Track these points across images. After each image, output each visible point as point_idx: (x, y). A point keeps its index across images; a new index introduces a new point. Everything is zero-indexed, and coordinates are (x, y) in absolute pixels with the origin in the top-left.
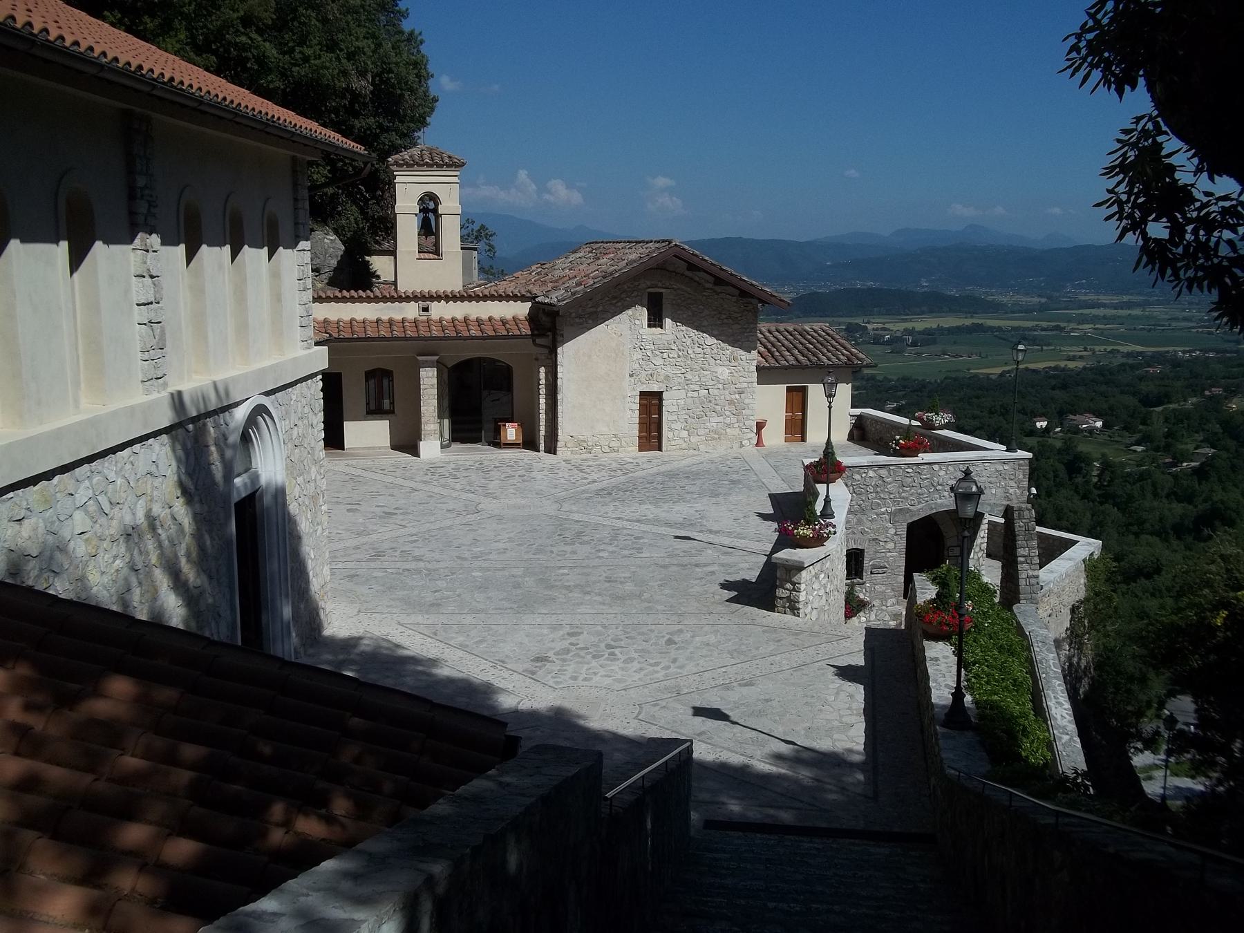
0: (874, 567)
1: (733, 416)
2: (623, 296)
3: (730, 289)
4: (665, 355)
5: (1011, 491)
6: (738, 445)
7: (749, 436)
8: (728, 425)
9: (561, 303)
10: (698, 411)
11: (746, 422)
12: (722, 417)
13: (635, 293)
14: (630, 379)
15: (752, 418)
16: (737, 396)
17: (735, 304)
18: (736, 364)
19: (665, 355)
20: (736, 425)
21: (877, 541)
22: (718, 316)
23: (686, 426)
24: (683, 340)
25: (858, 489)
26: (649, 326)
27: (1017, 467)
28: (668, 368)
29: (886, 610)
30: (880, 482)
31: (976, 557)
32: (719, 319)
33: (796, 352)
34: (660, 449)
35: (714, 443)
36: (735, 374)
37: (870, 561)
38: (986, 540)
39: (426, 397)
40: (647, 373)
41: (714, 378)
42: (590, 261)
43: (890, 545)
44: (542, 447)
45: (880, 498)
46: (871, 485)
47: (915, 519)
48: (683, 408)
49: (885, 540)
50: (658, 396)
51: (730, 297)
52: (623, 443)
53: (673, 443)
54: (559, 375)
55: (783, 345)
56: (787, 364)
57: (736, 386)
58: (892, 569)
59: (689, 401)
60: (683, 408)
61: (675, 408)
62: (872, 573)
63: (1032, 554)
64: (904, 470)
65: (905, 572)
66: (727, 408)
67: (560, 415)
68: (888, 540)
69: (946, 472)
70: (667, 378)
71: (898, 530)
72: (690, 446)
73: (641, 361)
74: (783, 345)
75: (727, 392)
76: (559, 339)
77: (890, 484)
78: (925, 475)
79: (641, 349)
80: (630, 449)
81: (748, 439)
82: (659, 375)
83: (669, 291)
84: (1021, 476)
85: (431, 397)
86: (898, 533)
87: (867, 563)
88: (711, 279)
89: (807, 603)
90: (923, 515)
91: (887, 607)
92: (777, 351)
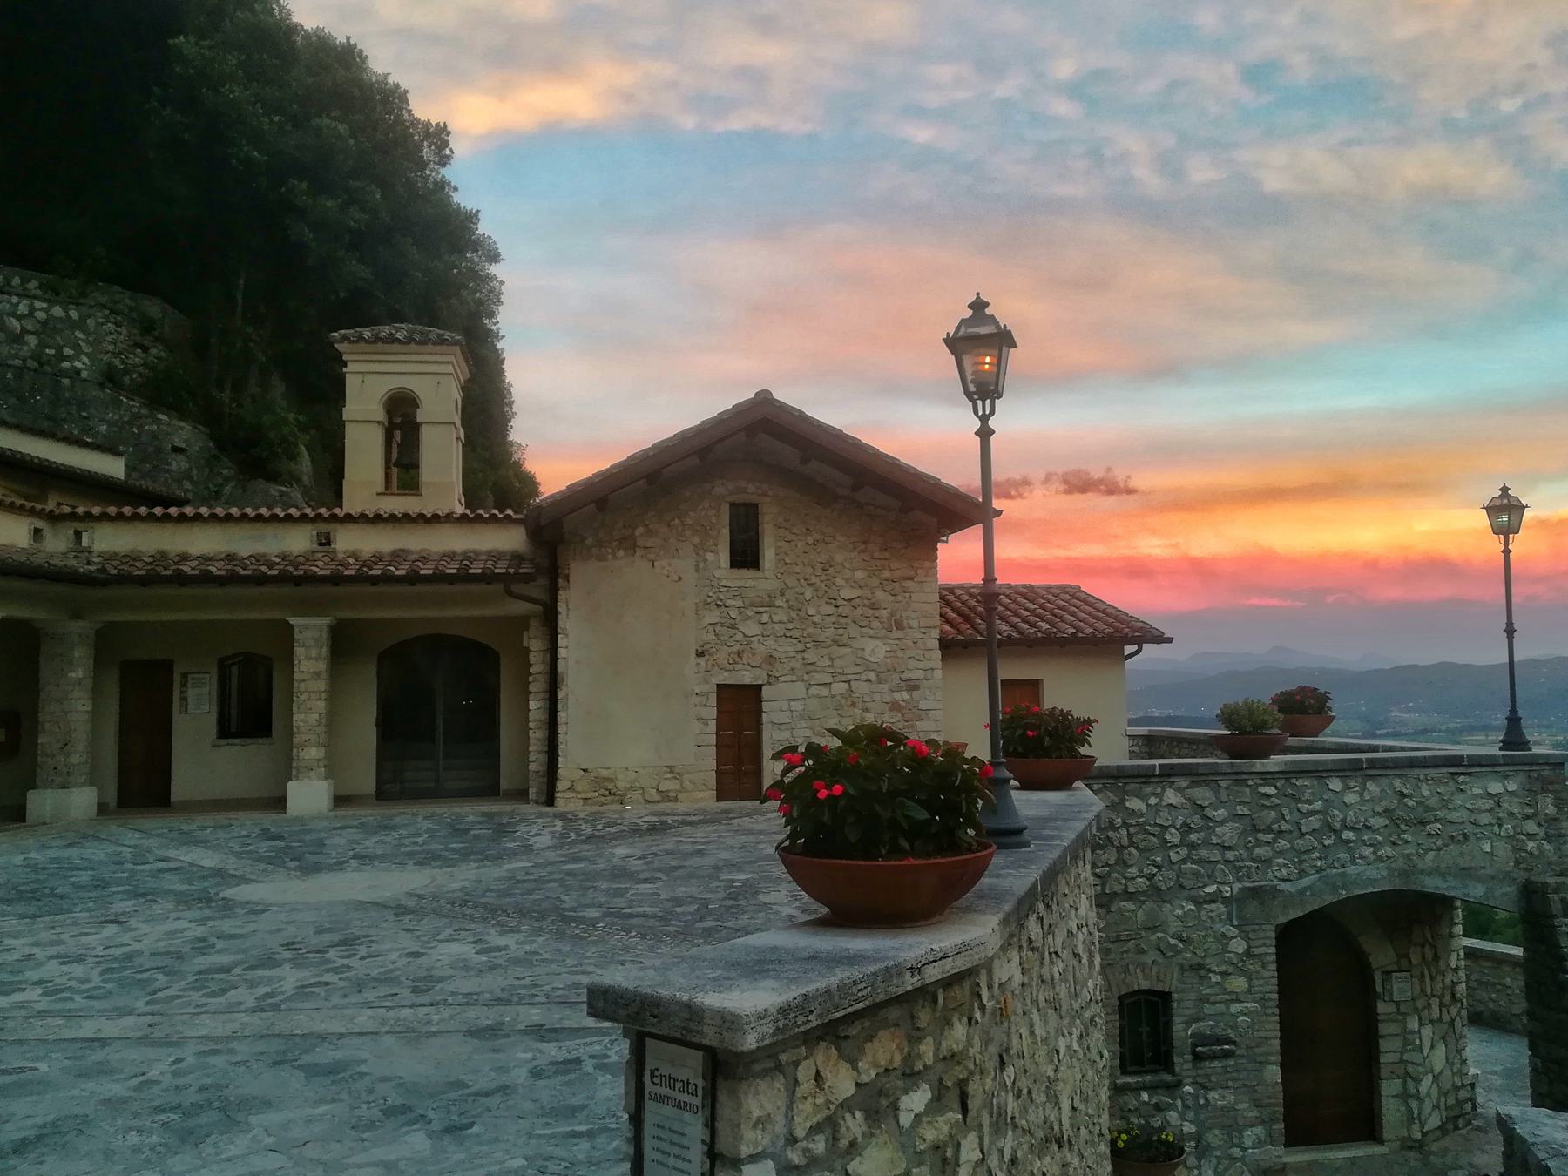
0: (1200, 1039)
4: (765, 618)
5: (1531, 845)
14: (699, 660)
16: (905, 695)
18: (900, 634)
19: (765, 618)
21: (1203, 973)
22: (862, 547)
24: (799, 590)
25: (1142, 836)
27: (1537, 786)
28: (770, 642)
29: (1242, 1159)
30: (1197, 818)
31: (1446, 1018)
36: (900, 654)
37: (1188, 1023)
38: (1462, 974)
40: (730, 650)
41: (859, 661)
43: (1239, 983)
44: (532, 792)
45: (1200, 861)
46: (1173, 826)
47: (1295, 914)
49: (1224, 968)
50: (752, 694)
52: (687, 784)
54: (562, 653)
60: (802, 717)
61: (783, 717)
62: (1198, 1058)
64: (1254, 788)
68: (1231, 970)
69: (1361, 794)
70: (770, 659)
71: (1252, 943)
73: (718, 628)
75: (885, 687)
76: (561, 582)
77: (1222, 823)
78: (1309, 802)
80: (701, 795)
82: (754, 654)
84: (1551, 810)
85: (313, 696)
86: (1256, 951)
87: (1182, 1032)
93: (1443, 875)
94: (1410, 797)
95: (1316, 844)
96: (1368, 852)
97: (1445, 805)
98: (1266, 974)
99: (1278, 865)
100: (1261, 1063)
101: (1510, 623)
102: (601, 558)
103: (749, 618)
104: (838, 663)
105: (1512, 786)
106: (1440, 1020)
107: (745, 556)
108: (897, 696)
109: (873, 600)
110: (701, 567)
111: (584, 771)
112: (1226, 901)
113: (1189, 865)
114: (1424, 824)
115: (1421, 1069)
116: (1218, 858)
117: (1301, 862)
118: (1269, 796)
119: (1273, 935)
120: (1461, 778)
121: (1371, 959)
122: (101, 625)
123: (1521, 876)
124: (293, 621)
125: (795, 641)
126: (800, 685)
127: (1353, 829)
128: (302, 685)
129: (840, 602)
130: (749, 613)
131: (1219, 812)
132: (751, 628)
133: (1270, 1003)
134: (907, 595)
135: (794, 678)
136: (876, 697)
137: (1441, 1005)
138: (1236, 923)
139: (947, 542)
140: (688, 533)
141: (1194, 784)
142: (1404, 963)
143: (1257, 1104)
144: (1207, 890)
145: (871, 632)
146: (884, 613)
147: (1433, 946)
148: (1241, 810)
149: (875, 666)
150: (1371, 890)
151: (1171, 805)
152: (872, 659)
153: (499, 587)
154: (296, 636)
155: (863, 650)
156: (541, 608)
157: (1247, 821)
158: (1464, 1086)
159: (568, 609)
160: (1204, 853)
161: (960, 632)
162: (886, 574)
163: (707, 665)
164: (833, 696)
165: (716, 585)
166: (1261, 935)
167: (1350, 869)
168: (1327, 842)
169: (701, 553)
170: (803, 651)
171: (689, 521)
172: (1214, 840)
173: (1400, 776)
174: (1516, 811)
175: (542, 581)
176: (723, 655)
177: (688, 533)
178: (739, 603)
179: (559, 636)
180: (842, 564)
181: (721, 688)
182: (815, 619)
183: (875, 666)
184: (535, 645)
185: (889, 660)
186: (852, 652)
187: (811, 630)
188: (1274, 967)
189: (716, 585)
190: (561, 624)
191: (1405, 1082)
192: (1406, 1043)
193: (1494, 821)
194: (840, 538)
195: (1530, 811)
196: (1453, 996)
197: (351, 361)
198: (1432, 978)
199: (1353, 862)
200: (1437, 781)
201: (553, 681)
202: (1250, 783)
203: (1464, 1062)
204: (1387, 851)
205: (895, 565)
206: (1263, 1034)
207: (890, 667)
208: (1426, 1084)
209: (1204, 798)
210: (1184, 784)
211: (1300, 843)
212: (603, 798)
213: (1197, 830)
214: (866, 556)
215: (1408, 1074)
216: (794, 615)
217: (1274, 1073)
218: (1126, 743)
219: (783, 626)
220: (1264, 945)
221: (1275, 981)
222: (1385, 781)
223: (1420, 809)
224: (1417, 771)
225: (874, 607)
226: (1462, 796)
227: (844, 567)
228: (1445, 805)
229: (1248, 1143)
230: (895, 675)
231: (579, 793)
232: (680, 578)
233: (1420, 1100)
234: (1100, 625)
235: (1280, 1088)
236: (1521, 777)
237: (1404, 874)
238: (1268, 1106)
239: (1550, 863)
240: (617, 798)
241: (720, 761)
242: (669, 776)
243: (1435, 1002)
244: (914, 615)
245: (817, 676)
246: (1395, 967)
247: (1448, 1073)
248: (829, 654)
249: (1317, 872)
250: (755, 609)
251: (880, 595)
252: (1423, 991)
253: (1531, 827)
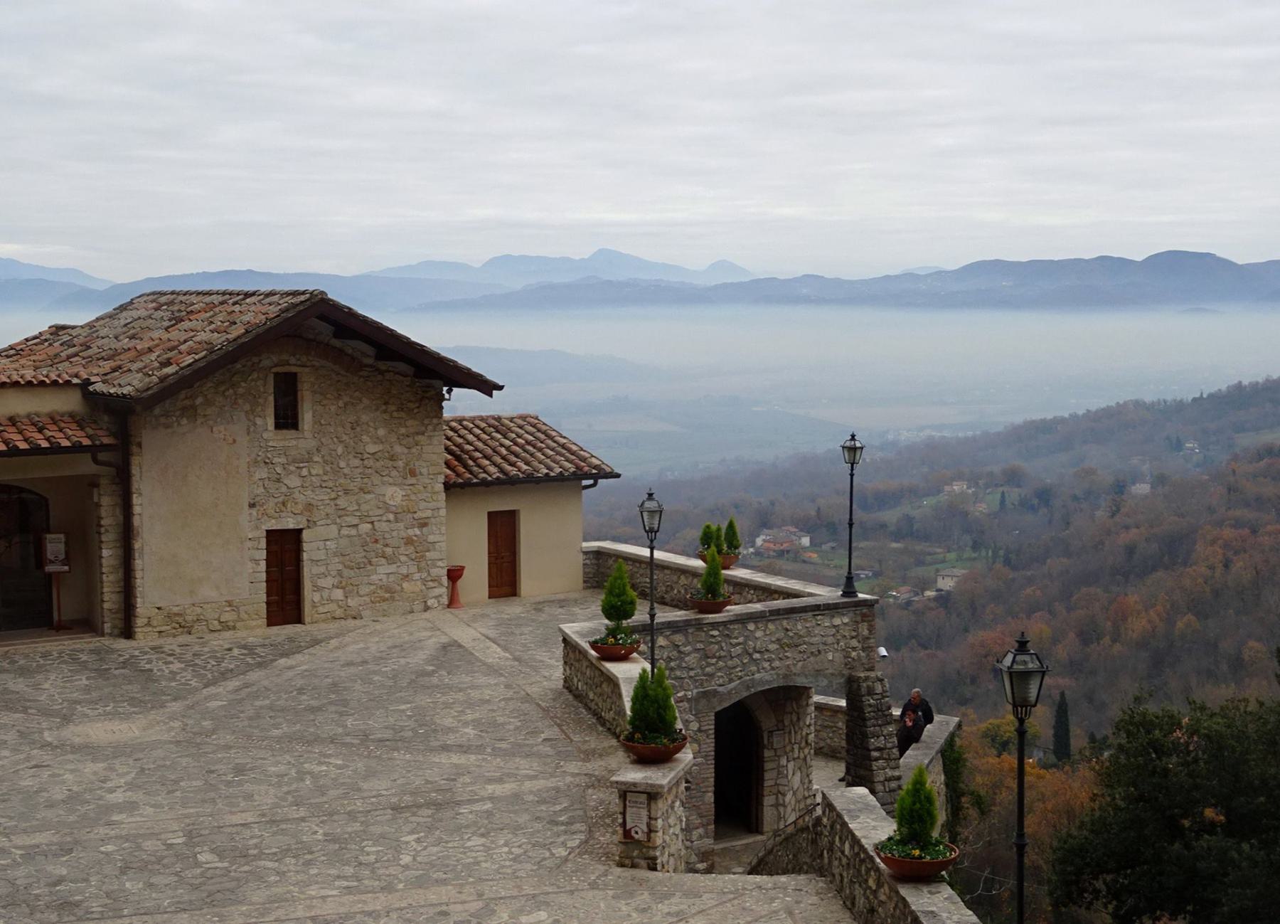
1: (412, 563)
2: (234, 379)
3: (402, 366)
4: (305, 472)
5: (854, 654)
6: (421, 607)
7: (437, 591)
8: (406, 577)
9: (144, 394)
10: (359, 556)
11: (431, 571)
12: (395, 566)
13: (255, 375)
14: (251, 511)
15: (440, 563)
16: (417, 531)
17: (408, 389)
18: (413, 481)
19: (305, 472)
20: (417, 576)
22: (384, 407)
23: (341, 582)
26: (278, 426)
27: (859, 619)
30: (675, 653)
31: (802, 756)
32: (385, 412)
33: (498, 460)
34: (299, 619)
35: (385, 605)
36: (413, 497)
40: (276, 500)
42: (166, 324)
45: (677, 678)
46: (662, 658)
47: (726, 705)
48: (335, 554)
51: (401, 378)
53: (321, 609)
54: (137, 509)
55: (476, 450)
56: (490, 478)
57: (415, 516)
58: (697, 784)
59: (344, 542)
60: (335, 554)
61: (321, 555)
63: (889, 745)
65: (715, 786)
66: (402, 550)
67: (138, 574)
69: (765, 631)
70: (309, 507)
71: (702, 724)
72: (348, 612)
73: (266, 482)
74: (476, 450)
75: (401, 525)
76: (135, 449)
77: (689, 654)
79: (266, 463)
80: (254, 623)
81: (436, 597)
82: (296, 503)
83: (307, 370)
84: (866, 632)
86: (703, 728)
88: (370, 350)
89: (664, 847)
90: (735, 699)
91: (692, 842)
92: (470, 458)
93: (806, 676)
94: (791, 630)
95: (739, 663)
96: (766, 665)
97: (809, 634)
98: (708, 741)
99: (718, 677)
100: (704, 792)
101: (851, 519)
102: (167, 426)
103: (292, 472)
104: (364, 507)
105: (846, 620)
106: (799, 758)
107: (287, 419)
108: (410, 532)
109: (392, 453)
110: (252, 430)
111: (159, 608)
112: (689, 700)
113: (670, 681)
114: (797, 646)
115: (786, 788)
116: (686, 675)
117: (730, 674)
118: (713, 636)
119: (713, 718)
120: (819, 617)
121: (763, 724)
123: (846, 672)
125: (329, 490)
126: (334, 528)
127: (759, 652)
129: (366, 456)
130: (292, 468)
131: (687, 648)
132: (293, 481)
133: (711, 758)
134: (419, 448)
135: (329, 522)
136: (395, 534)
137: (800, 748)
138: (694, 713)
139: (449, 400)
140: (240, 401)
141: (674, 632)
142: (780, 726)
143: (701, 816)
144: (679, 695)
145: (391, 480)
146: (400, 464)
147: (798, 714)
148: (700, 646)
149: (394, 508)
150: (767, 687)
151: (661, 646)
152: (391, 503)
155: (384, 495)
156: (113, 470)
157: (702, 652)
158: (810, 796)
159: (141, 472)
160: (678, 673)
161: (458, 475)
162: (403, 430)
163: (258, 514)
164: (360, 536)
165: (264, 446)
166: (707, 719)
167: (757, 676)
168: (745, 661)
169: (252, 417)
170: (335, 499)
171: (241, 391)
172: (684, 665)
173: (786, 618)
174: (847, 634)
176: (270, 506)
177: (240, 401)
178: (283, 460)
179: (135, 496)
180: (367, 423)
181: (267, 531)
182: (346, 471)
183: (394, 508)
185: (404, 503)
186: (376, 498)
187: (342, 481)
188: (713, 736)
189: (264, 446)
190: (135, 486)
191: (777, 798)
192: (779, 773)
193: (835, 641)
194: (366, 401)
195: (854, 634)
196: (807, 742)
198: (796, 732)
199: (759, 671)
200: (805, 620)
201: (127, 535)
202: (705, 629)
203: (810, 782)
204: (777, 664)
205: (410, 423)
206: (706, 776)
207: (405, 509)
208: (789, 797)
209: (680, 641)
210: (668, 633)
211: (730, 663)
212: (174, 631)
213: (675, 660)
214: (386, 416)
215: (779, 792)
216: (328, 468)
217: (710, 797)
218: (581, 557)
219: (318, 478)
220: (708, 724)
221: (713, 745)
222: (778, 622)
223: (796, 637)
224: (795, 615)
225: (392, 458)
226: (819, 628)
227: (369, 426)
228: (809, 634)
229: (694, 838)
230: (410, 515)
231: (155, 627)
232: (234, 441)
233: (785, 806)
234: (567, 465)
235: (713, 805)
236: (851, 614)
237: (785, 676)
238: (706, 816)
239: (863, 664)
240: (186, 630)
241: (269, 594)
242: (228, 609)
243: (796, 747)
244: (424, 464)
245: (348, 519)
246: (776, 728)
247: (801, 789)
248: (356, 501)
249: (739, 679)
250: (297, 465)
251: (398, 449)
252: (790, 740)
253: (854, 643)
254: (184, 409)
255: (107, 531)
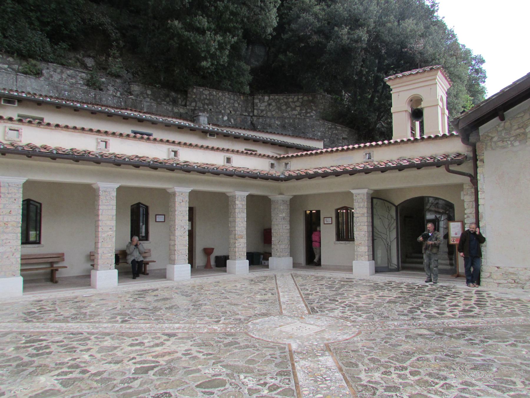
39: (359, 224)
54: (481, 202)
85: (362, 224)
102: (503, 147)
111: (498, 268)
122: (292, 197)
124: (353, 191)
128: (357, 219)
153: (442, 169)
154: (354, 198)
175: (470, 164)
179: (479, 193)
184: (468, 199)
197: (394, 88)
212: (510, 284)
231: (495, 280)
240: (520, 285)
254: (517, 136)
255: (468, 217)
